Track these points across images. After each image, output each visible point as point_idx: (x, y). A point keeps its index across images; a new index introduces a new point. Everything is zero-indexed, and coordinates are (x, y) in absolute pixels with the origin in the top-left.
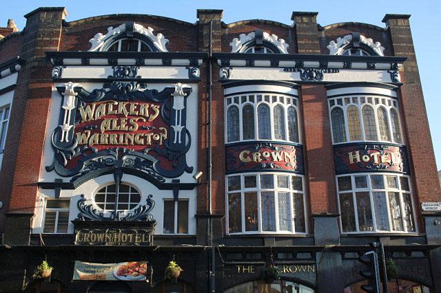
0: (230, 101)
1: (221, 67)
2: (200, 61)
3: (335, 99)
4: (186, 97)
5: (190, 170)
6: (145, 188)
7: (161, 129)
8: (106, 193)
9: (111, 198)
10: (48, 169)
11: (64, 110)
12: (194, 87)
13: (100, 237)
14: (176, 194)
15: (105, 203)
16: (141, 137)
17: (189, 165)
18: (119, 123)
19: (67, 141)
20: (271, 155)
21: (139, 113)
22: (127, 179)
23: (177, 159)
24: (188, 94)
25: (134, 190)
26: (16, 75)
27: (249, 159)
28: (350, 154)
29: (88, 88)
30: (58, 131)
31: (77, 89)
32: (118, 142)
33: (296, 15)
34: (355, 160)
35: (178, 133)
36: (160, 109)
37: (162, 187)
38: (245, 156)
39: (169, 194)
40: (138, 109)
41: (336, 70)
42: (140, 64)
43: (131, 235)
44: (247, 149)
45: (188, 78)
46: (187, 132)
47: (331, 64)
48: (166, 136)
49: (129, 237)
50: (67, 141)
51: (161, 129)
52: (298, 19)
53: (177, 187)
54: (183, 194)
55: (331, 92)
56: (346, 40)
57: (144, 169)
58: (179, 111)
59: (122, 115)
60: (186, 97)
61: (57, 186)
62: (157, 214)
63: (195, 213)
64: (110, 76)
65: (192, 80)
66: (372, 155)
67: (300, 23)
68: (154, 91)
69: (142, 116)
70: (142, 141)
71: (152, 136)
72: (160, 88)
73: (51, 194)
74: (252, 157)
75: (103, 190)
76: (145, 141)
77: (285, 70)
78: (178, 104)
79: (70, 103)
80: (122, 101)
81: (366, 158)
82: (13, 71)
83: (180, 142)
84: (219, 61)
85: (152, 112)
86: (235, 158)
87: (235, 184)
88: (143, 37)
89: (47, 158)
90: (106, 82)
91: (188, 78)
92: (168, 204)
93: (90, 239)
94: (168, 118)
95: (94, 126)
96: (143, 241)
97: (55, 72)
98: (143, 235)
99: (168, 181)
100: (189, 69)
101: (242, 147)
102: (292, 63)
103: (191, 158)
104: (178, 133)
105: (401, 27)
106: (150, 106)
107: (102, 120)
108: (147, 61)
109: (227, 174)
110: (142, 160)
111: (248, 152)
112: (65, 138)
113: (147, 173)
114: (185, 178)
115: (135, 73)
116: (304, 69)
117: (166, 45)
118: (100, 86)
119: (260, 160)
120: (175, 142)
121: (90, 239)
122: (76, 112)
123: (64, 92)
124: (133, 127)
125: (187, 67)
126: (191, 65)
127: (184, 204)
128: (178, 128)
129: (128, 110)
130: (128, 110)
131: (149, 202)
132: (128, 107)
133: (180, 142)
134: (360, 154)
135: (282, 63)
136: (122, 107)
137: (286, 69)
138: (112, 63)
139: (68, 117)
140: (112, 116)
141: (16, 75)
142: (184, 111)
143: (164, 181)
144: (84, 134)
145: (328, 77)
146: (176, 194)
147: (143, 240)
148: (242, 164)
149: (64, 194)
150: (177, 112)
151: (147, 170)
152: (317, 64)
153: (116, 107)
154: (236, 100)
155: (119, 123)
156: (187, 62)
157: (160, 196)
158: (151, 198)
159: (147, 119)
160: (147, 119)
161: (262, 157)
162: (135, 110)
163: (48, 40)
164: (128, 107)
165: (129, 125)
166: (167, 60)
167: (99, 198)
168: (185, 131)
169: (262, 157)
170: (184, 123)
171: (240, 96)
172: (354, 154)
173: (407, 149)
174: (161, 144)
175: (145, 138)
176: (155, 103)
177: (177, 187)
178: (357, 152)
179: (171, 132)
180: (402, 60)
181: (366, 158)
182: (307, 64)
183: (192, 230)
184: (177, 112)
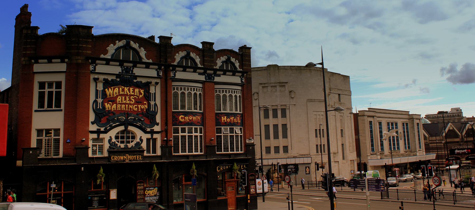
0: (174, 89)
1: (171, 71)
2: (163, 67)
3: (218, 90)
4: (155, 86)
5: (158, 124)
6: (139, 133)
7: (145, 102)
8: (120, 135)
9: (122, 138)
10: (93, 123)
11: (98, 90)
12: (158, 81)
13: (122, 158)
14: (152, 136)
15: (120, 140)
16: (136, 107)
17: (157, 122)
18: (125, 99)
19: (101, 108)
20: (192, 118)
21: (135, 94)
22: (130, 128)
23: (152, 119)
24: (157, 85)
25: (132, 133)
26: (65, 65)
27: (183, 120)
28: (223, 117)
29: (110, 78)
30: (95, 102)
31: (104, 79)
32: (126, 109)
33: (203, 43)
34: (224, 121)
35: (152, 105)
36: (144, 92)
37: (146, 132)
38: (182, 118)
39: (149, 136)
40: (134, 92)
41: (219, 76)
42: (135, 66)
43: (135, 156)
44: (182, 115)
45: (156, 76)
46: (156, 105)
47: (218, 73)
48: (146, 106)
49: (134, 157)
50: (101, 108)
51: (145, 102)
52: (205, 45)
53: (152, 132)
54: (155, 136)
55: (217, 86)
56: (223, 59)
57: (138, 123)
58: (152, 93)
59: (127, 95)
60: (155, 86)
61: (98, 132)
62: (144, 145)
63: (160, 146)
64: (120, 73)
65: (159, 77)
66: (231, 119)
67: (206, 48)
68: (141, 82)
69: (135, 96)
70: (136, 109)
71: (141, 107)
72: (144, 81)
73: (95, 136)
74: (185, 119)
75: (118, 133)
76: (138, 109)
77: (198, 74)
78: (152, 90)
79: (100, 87)
80: (125, 87)
81: (229, 120)
82: (63, 62)
83: (154, 110)
84: (171, 68)
85: (140, 93)
86: (177, 119)
87: (176, 131)
88: (134, 50)
89: (92, 117)
90: (117, 76)
91: (156, 76)
92: (148, 140)
93: (117, 159)
94: (148, 97)
95: (113, 100)
96: (140, 159)
97: (91, 68)
98: (140, 156)
99: (149, 130)
100: (157, 71)
101: (180, 114)
102: (202, 71)
103: (158, 119)
104: (152, 105)
105: (247, 53)
106: (139, 90)
107: (117, 96)
108: (138, 65)
109: (173, 126)
110: (137, 119)
111: (183, 116)
112: (100, 106)
113: (139, 125)
114: (157, 128)
115: (132, 71)
116: (207, 74)
117: (145, 54)
118: (114, 78)
119: (188, 120)
120: (151, 110)
121: (117, 159)
122: (104, 92)
123: (98, 80)
124: (132, 102)
125: (156, 70)
126: (158, 69)
127: (155, 140)
128: (152, 103)
129: (130, 92)
130: (130, 92)
131: (141, 140)
132: (129, 90)
133: (154, 110)
134: (226, 118)
135: (198, 71)
136: (126, 89)
137: (200, 74)
138: (121, 65)
139: (100, 94)
140: (122, 95)
141: (65, 65)
142: (155, 93)
143: (147, 129)
144: (109, 105)
145: (217, 79)
146: (152, 136)
147: (140, 158)
148: (181, 122)
149: (102, 136)
150: (152, 94)
151: (138, 124)
152: (212, 72)
153: (123, 90)
154: (177, 89)
155: (125, 99)
156: (157, 67)
157: (145, 137)
158: (142, 138)
159: (138, 97)
160: (138, 97)
161: (189, 119)
162: (133, 92)
163: (85, 47)
164: (129, 90)
165: (130, 100)
166: (147, 66)
167: (117, 137)
168: (156, 105)
169: (189, 119)
170: (155, 100)
171: (179, 87)
172: (224, 118)
173: (243, 115)
174: (145, 111)
175: (138, 107)
176: (142, 88)
177: (152, 132)
178: (225, 117)
179: (149, 105)
180: (246, 73)
181: (229, 120)
182: (209, 72)
183: (159, 152)
184: (152, 94)
